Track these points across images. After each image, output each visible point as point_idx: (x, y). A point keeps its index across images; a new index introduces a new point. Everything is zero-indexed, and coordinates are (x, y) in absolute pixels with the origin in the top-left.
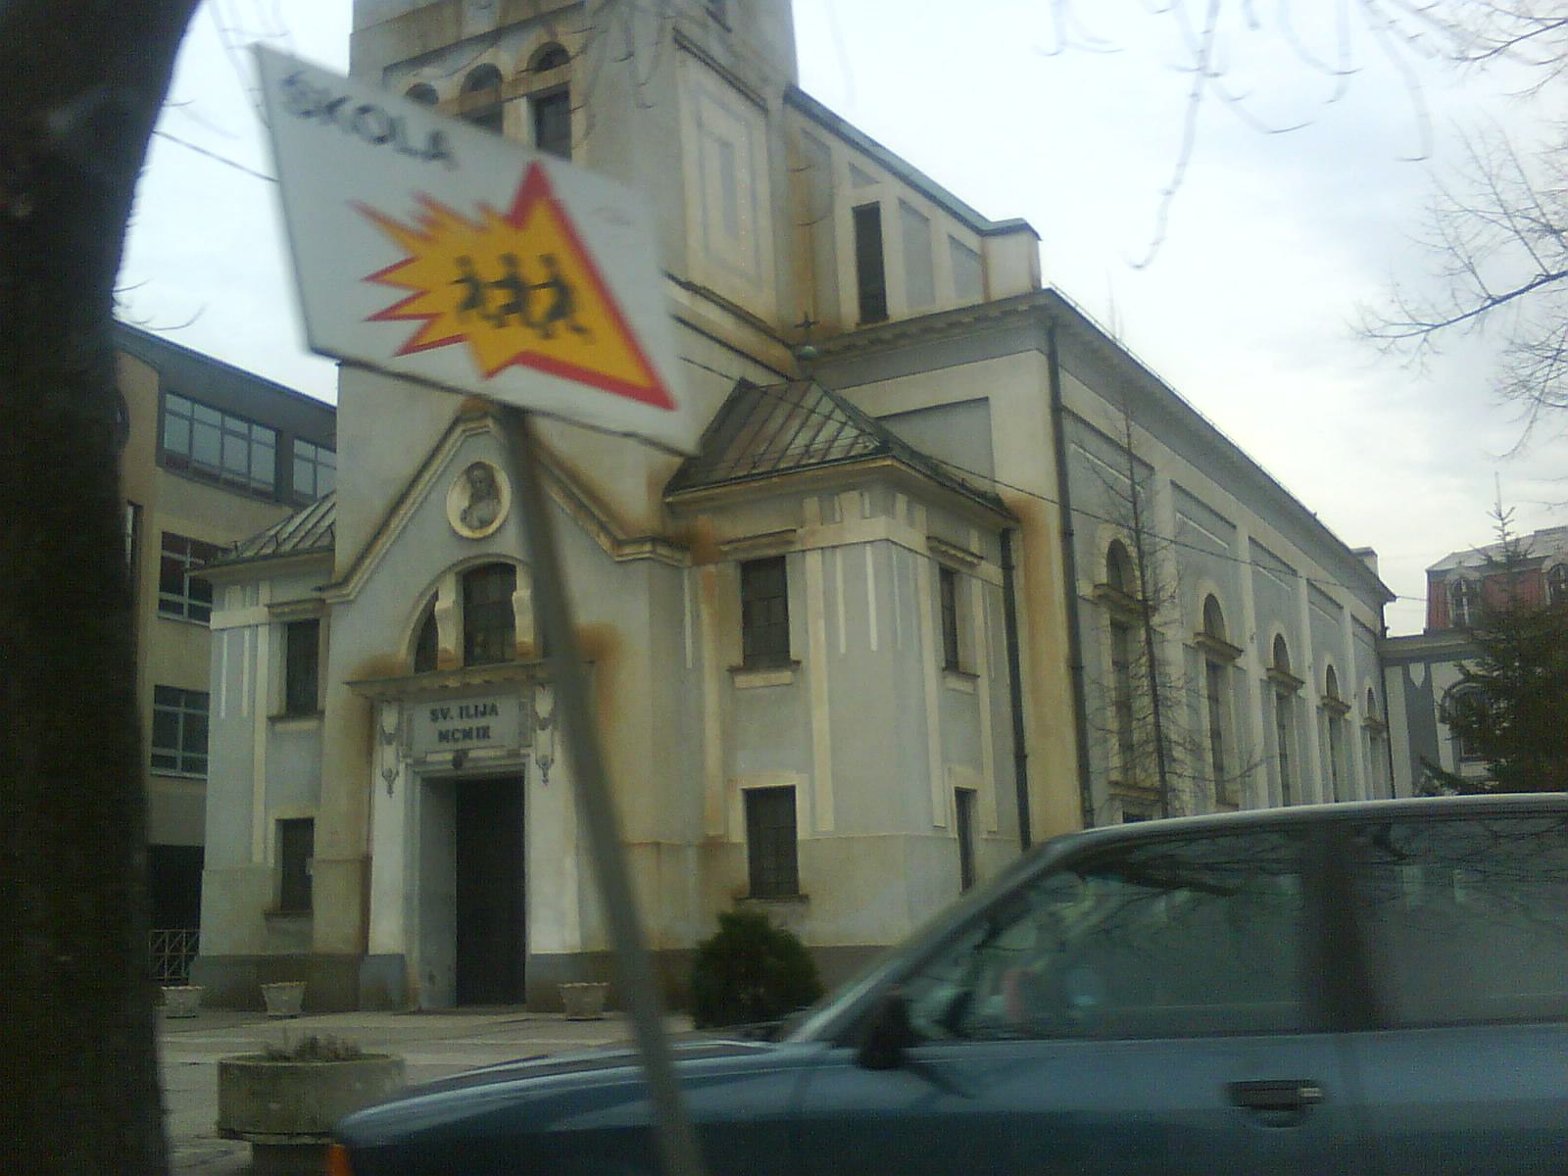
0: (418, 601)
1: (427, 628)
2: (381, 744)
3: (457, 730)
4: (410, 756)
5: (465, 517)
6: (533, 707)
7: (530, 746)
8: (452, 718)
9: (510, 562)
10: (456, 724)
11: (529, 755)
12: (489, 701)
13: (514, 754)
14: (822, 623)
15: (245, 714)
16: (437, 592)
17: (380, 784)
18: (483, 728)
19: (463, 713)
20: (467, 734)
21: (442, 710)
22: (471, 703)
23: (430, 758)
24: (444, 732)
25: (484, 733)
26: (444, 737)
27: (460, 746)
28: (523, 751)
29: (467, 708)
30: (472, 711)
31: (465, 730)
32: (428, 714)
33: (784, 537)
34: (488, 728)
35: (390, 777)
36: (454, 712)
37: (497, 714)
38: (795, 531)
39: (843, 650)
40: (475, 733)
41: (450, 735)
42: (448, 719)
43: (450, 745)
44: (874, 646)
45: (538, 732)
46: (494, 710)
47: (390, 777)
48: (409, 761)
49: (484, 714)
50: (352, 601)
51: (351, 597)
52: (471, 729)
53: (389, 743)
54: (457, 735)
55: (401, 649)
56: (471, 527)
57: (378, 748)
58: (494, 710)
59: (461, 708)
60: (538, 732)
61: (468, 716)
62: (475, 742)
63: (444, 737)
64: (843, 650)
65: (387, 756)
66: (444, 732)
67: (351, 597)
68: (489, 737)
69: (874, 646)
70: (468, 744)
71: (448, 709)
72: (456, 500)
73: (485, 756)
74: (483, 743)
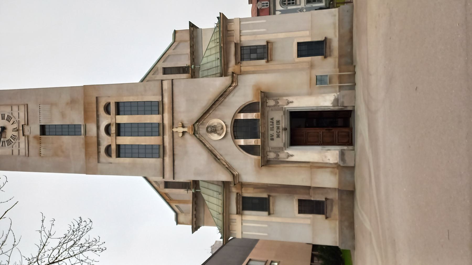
0: (240, 151)
1: (248, 149)
2: (279, 159)
3: (277, 131)
4: (283, 148)
5: (220, 135)
6: (272, 106)
7: (283, 107)
8: (273, 133)
9: (233, 121)
10: (274, 133)
11: (285, 108)
12: (270, 120)
14: (258, 36)
15: (266, 226)
16: (238, 145)
18: (277, 123)
19: (272, 129)
20: (278, 128)
21: (271, 137)
22: (270, 127)
23: (284, 141)
24: (277, 136)
25: (278, 122)
26: (278, 136)
27: (281, 130)
28: (284, 110)
29: (271, 128)
30: (272, 126)
31: (277, 129)
32: (272, 141)
33: (236, 45)
34: (277, 121)
35: (289, 156)
37: (273, 118)
38: (235, 43)
39: (264, 30)
40: (278, 126)
41: (277, 134)
42: (273, 135)
43: (281, 134)
44: (265, 21)
45: (278, 104)
46: (272, 119)
48: (284, 148)
49: (273, 123)
50: (238, 174)
51: (237, 174)
52: (277, 127)
53: (278, 155)
54: (278, 132)
55: (252, 159)
56: (223, 132)
57: (280, 160)
58: (272, 119)
59: (271, 130)
60: (278, 104)
61: (273, 128)
62: (280, 126)
63: (278, 136)
64: (264, 30)
65: (282, 156)
66: (277, 136)
67: (237, 174)
68: (279, 121)
69: (265, 21)
70: (281, 128)
71: (271, 135)
72: (215, 137)
73: (285, 122)
74: (281, 122)
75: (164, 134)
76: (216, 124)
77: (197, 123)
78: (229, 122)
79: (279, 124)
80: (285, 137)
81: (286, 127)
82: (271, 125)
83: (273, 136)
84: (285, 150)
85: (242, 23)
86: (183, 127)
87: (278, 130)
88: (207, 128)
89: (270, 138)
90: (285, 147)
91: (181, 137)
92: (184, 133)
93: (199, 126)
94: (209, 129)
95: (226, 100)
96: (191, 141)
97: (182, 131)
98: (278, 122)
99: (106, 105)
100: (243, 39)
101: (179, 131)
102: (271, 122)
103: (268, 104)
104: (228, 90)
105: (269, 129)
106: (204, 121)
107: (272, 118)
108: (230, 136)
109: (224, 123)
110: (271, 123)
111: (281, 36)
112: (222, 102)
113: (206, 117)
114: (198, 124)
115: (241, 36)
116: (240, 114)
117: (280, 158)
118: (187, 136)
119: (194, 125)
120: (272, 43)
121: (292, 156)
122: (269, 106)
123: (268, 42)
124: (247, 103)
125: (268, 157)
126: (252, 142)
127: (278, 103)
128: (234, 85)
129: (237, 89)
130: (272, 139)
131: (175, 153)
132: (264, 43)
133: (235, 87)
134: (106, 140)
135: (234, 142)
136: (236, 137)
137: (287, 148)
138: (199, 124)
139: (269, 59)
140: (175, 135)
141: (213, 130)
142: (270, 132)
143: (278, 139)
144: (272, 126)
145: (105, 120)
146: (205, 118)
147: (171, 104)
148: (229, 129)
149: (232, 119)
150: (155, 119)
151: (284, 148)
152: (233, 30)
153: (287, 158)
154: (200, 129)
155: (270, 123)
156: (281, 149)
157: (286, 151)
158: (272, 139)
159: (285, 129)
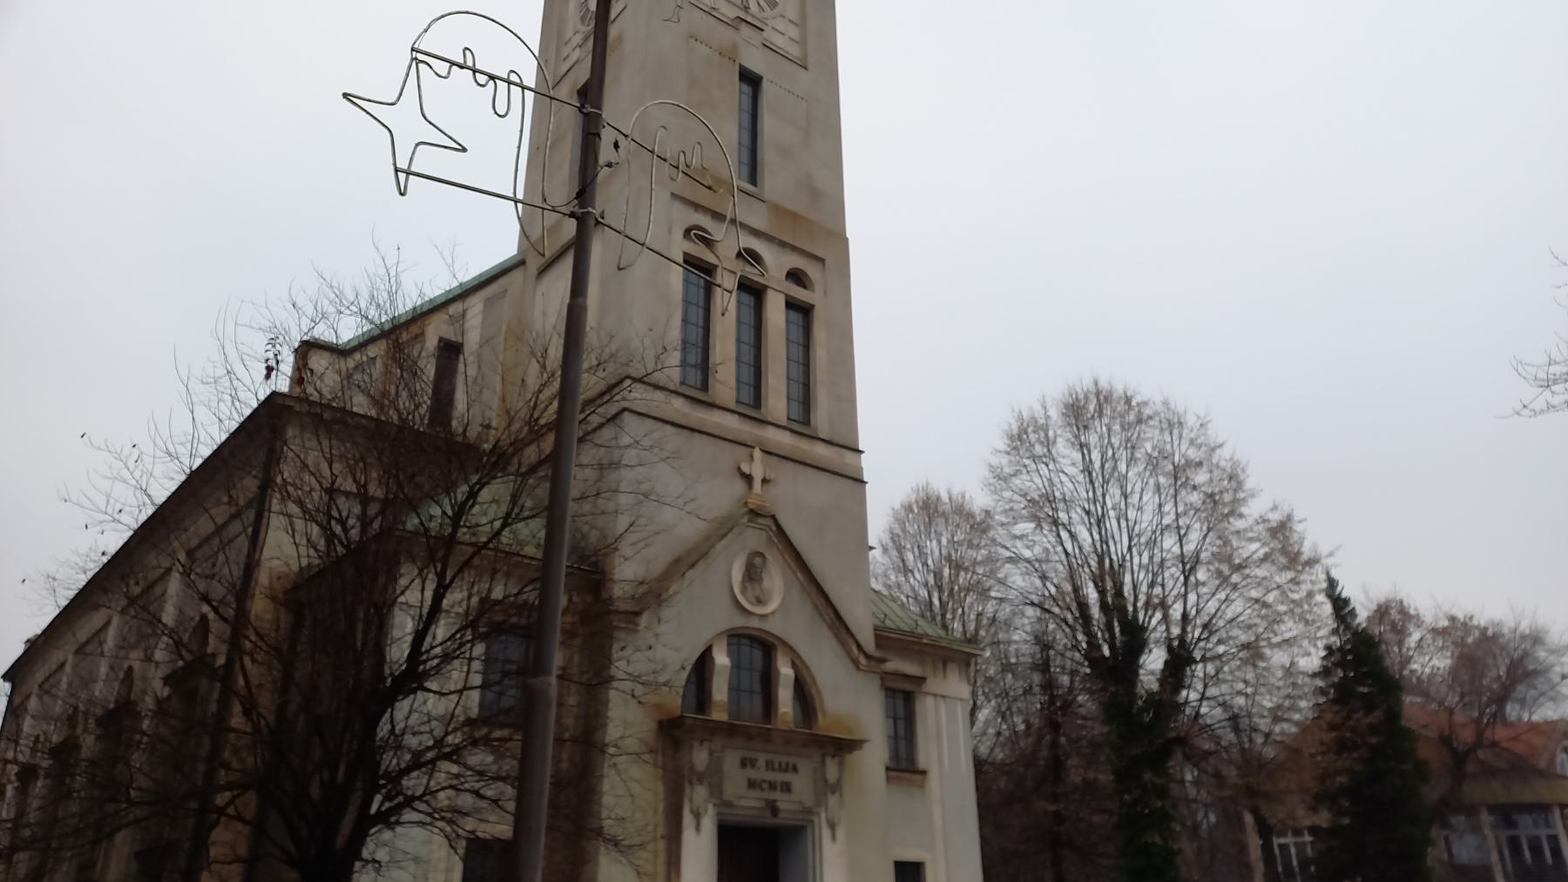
3: (764, 781)
10: (761, 774)
12: (792, 760)
13: (808, 811)
17: (688, 819)
19: (770, 765)
20: (772, 786)
22: (777, 759)
26: (752, 784)
30: (776, 765)
32: (737, 762)
35: (697, 816)
36: (761, 762)
40: (779, 788)
43: (756, 793)
46: (795, 769)
47: (697, 816)
49: (786, 770)
53: (700, 781)
58: (795, 769)
61: (773, 770)
63: (752, 784)
65: (699, 794)
75: (743, 419)
76: (766, 583)
77: (774, 528)
78: (774, 627)
79: (782, 790)
80: (749, 805)
81: (781, 815)
82: (780, 764)
83: (753, 766)
84: (715, 805)
85: (959, 703)
86: (765, 481)
87: (765, 786)
88: (761, 555)
89: (749, 754)
90: (723, 804)
91: (739, 469)
92: (748, 478)
93: (764, 533)
94: (758, 560)
95: (826, 633)
96: (721, 496)
97: (753, 474)
98: (787, 788)
99: (804, 279)
100: (929, 701)
101: (754, 464)
102: (787, 764)
103: (828, 760)
104: (850, 641)
105: (770, 757)
106: (778, 549)
107: (799, 766)
108: (738, 621)
109: (773, 613)
110: (784, 766)
111: (937, 811)
112: (822, 616)
113: (789, 560)
114: (771, 529)
115: (935, 699)
116: (790, 664)
117: (692, 788)
118: (739, 486)
119: (773, 517)
120: (921, 786)
121: (698, 827)
122: (823, 762)
123: (924, 773)
124: (819, 693)
125: (696, 744)
126: (720, 690)
127: (833, 793)
128: (863, 660)
129: (851, 666)
130: (744, 764)
131: (697, 435)
132: (922, 761)
133: (855, 662)
134: (728, 243)
135: (719, 635)
136: (737, 638)
137: (718, 814)
138: (771, 533)
139: (892, 774)
140: (743, 451)
141: (752, 574)
142: (762, 759)
143: (744, 784)
144: (776, 765)
145: (776, 263)
146: (786, 556)
147: (814, 464)
148: (755, 623)
149: (780, 639)
150: (777, 403)
151: (718, 801)
152: (945, 677)
153: (692, 811)
154: (756, 531)
155: (784, 759)
156: (716, 791)
157: (710, 807)
158: (744, 764)
159: (773, 808)
